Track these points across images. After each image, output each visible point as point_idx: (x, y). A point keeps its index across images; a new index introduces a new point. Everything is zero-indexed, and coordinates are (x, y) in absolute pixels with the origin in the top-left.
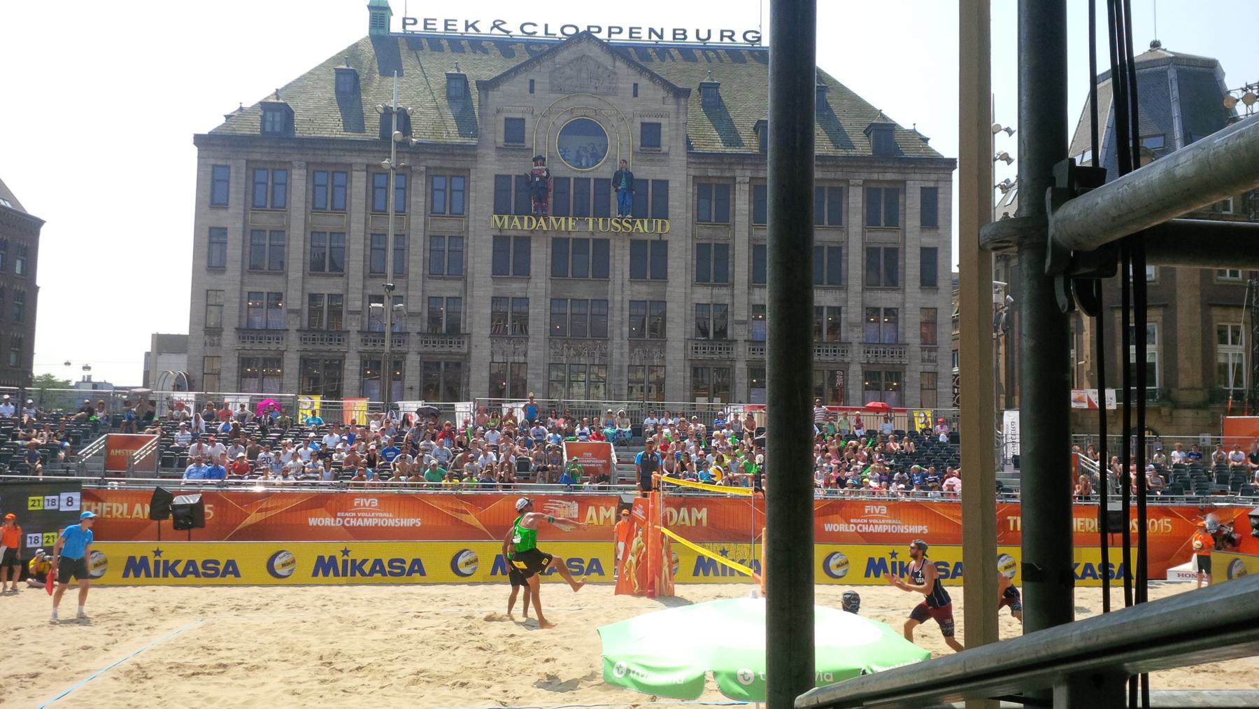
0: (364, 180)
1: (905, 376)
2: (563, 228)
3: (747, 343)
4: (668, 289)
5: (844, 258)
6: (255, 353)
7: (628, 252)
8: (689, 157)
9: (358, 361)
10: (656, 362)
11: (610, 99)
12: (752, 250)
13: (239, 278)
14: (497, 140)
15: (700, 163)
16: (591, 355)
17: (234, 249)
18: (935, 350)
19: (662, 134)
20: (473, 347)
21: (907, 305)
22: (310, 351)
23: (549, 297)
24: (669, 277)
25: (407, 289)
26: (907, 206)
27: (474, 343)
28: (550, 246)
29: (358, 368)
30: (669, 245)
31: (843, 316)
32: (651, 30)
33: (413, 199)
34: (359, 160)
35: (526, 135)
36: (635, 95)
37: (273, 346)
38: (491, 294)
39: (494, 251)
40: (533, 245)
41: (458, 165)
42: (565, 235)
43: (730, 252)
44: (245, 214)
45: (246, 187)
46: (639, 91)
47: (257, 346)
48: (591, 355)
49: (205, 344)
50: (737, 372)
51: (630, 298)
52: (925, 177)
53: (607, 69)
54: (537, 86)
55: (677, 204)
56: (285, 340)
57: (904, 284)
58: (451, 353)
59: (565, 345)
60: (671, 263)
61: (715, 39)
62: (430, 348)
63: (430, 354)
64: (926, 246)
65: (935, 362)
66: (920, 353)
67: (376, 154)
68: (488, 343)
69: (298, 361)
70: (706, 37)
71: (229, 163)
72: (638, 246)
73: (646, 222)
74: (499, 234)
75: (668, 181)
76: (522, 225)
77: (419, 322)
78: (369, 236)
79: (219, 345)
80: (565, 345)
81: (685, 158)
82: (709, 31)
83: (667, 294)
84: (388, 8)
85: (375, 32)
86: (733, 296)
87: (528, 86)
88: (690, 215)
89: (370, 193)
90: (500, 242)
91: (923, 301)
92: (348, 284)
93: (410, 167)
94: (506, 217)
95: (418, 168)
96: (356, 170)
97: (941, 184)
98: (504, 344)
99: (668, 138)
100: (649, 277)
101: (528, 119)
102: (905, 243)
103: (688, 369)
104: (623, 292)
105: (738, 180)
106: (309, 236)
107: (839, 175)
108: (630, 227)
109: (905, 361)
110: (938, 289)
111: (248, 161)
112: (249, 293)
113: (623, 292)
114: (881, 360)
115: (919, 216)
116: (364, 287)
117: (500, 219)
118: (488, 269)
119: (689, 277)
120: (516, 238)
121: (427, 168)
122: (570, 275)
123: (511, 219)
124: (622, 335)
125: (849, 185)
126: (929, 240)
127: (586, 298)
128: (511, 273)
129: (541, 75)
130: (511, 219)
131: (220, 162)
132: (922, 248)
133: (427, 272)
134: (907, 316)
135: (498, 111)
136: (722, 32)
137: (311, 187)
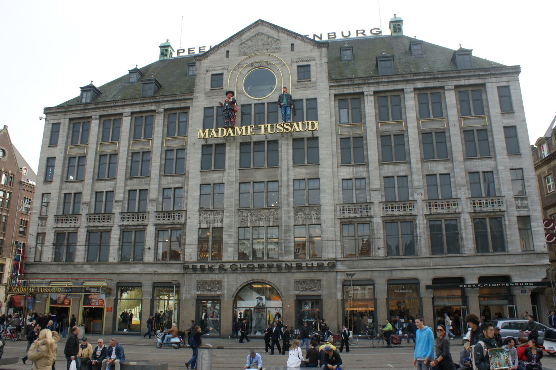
0: (129, 121)
1: (505, 220)
2: (244, 134)
3: (381, 204)
4: (320, 169)
5: (447, 139)
6: (63, 229)
7: (291, 147)
8: (331, 83)
9: (118, 232)
10: (314, 222)
11: (275, 55)
12: (380, 139)
13: (58, 186)
14: (206, 87)
15: (339, 86)
16: (267, 219)
17: (58, 170)
18: (526, 198)
19: (311, 71)
20: (188, 218)
21: (499, 168)
22: (93, 227)
23: (238, 181)
24: (321, 162)
25: (149, 184)
26: (489, 99)
27: (188, 216)
28: (239, 148)
29: (119, 237)
30: (320, 140)
31: (452, 180)
32: (315, 35)
33: (156, 129)
34: (127, 110)
35: (224, 83)
36: (292, 50)
37: (72, 225)
38: (199, 183)
39: (203, 155)
40: (227, 148)
41: (183, 105)
42: (249, 140)
43: (364, 142)
44: (66, 150)
45: (68, 133)
46: (295, 48)
47: (64, 225)
48: (267, 219)
49: (38, 225)
50: (375, 226)
51: (293, 178)
52: (500, 79)
53: (274, 38)
54: (230, 54)
55: (323, 112)
56: (79, 220)
57: (494, 152)
58: (174, 224)
59: (249, 214)
60: (321, 151)
61: (353, 35)
62: (161, 221)
63: (161, 225)
64: (507, 125)
65: (527, 207)
66: (514, 202)
67: (136, 106)
68: (197, 215)
69: (85, 233)
70: (348, 35)
71: (60, 122)
72: (297, 141)
73: (300, 123)
74: (205, 144)
75: (316, 99)
76: (217, 135)
77: (156, 204)
78: (130, 154)
79: (45, 226)
80: (249, 214)
81: (327, 83)
82: (349, 32)
83: (320, 173)
84: (169, 46)
85: (162, 58)
86: (368, 171)
87: (225, 54)
88: (334, 119)
89: (133, 129)
90: (206, 147)
91: (511, 164)
92: (116, 184)
93: (154, 111)
94: (207, 130)
95: (160, 110)
96: (125, 116)
97: (511, 84)
98: (207, 215)
99: (315, 73)
100: (306, 162)
101: (225, 72)
102: (491, 125)
103: (338, 226)
104: (288, 174)
105: (365, 94)
106: (98, 157)
107: (437, 84)
108: (289, 128)
109: (503, 208)
110: (521, 154)
111: (71, 120)
112: (65, 194)
113: (288, 174)
114: (485, 209)
115: (498, 106)
116: (126, 185)
117: (204, 132)
118: (198, 166)
119: (335, 161)
120: (217, 145)
121: (165, 110)
122: (252, 166)
123: (210, 132)
124: (288, 205)
125: (445, 90)
126: (509, 121)
127: (263, 180)
128: (213, 168)
129: (233, 48)
130: (210, 132)
131: (56, 122)
132: (505, 127)
133: (163, 173)
134: (500, 176)
135: (207, 71)
136: (357, 31)
137: (101, 130)
